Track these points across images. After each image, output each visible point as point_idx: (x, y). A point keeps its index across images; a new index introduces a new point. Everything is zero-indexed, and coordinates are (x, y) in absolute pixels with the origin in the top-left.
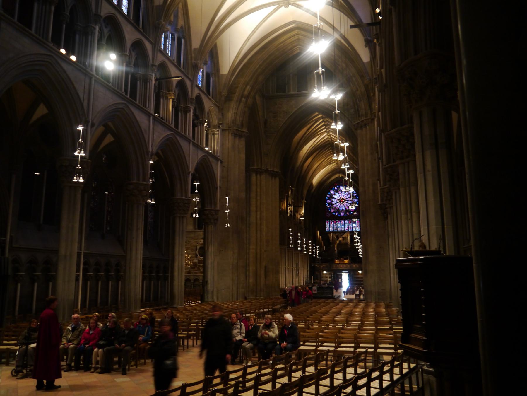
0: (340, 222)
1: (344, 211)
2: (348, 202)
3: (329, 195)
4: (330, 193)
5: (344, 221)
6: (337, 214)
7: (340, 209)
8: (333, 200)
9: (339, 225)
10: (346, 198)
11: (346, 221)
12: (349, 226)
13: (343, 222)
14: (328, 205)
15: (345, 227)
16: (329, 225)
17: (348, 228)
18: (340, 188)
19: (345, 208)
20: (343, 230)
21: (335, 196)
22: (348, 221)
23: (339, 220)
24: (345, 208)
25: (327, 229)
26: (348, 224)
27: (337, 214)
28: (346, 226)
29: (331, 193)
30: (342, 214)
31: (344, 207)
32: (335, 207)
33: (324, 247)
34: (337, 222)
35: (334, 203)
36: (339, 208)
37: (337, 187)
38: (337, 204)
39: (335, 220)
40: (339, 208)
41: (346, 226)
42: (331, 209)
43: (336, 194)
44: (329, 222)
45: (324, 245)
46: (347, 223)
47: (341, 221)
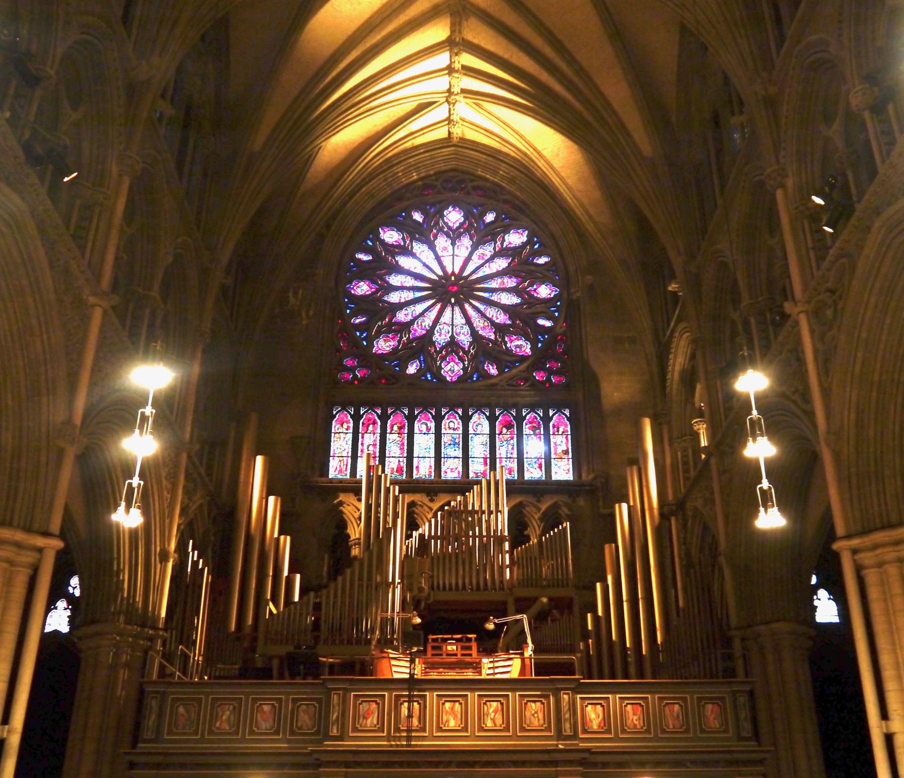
0: (432, 425)
1: (466, 353)
2: (495, 297)
3: (366, 251)
4: (377, 238)
5: (466, 419)
6: (412, 369)
7: (441, 338)
8: (395, 280)
9: (424, 443)
10: (480, 274)
11: (480, 423)
12: (501, 452)
13: (458, 424)
14: (355, 314)
15: (466, 458)
16: (350, 436)
17: (492, 460)
18: (442, 216)
19: (474, 332)
20: (452, 470)
21: (404, 262)
22: (492, 420)
23: (425, 408)
24: (474, 332)
25: (334, 464)
26: (492, 435)
27: (412, 369)
28: (478, 447)
29: (383, 243)
30: (452, 369)
31: (466, 329)
32: (406, 326)
33: (290, 582)
34: (411, 419)
35: (394, 298)
36: (431, 331)
37: (425, 213)
38: (420, 308)
39: (398, 408)
40: (431, 331)
41: (478, 447)
42: (377, 336)
43: (419, 248)
44: (356, 418)
45: (292, 571)
46: (485, 427)
47: (438, 419)
